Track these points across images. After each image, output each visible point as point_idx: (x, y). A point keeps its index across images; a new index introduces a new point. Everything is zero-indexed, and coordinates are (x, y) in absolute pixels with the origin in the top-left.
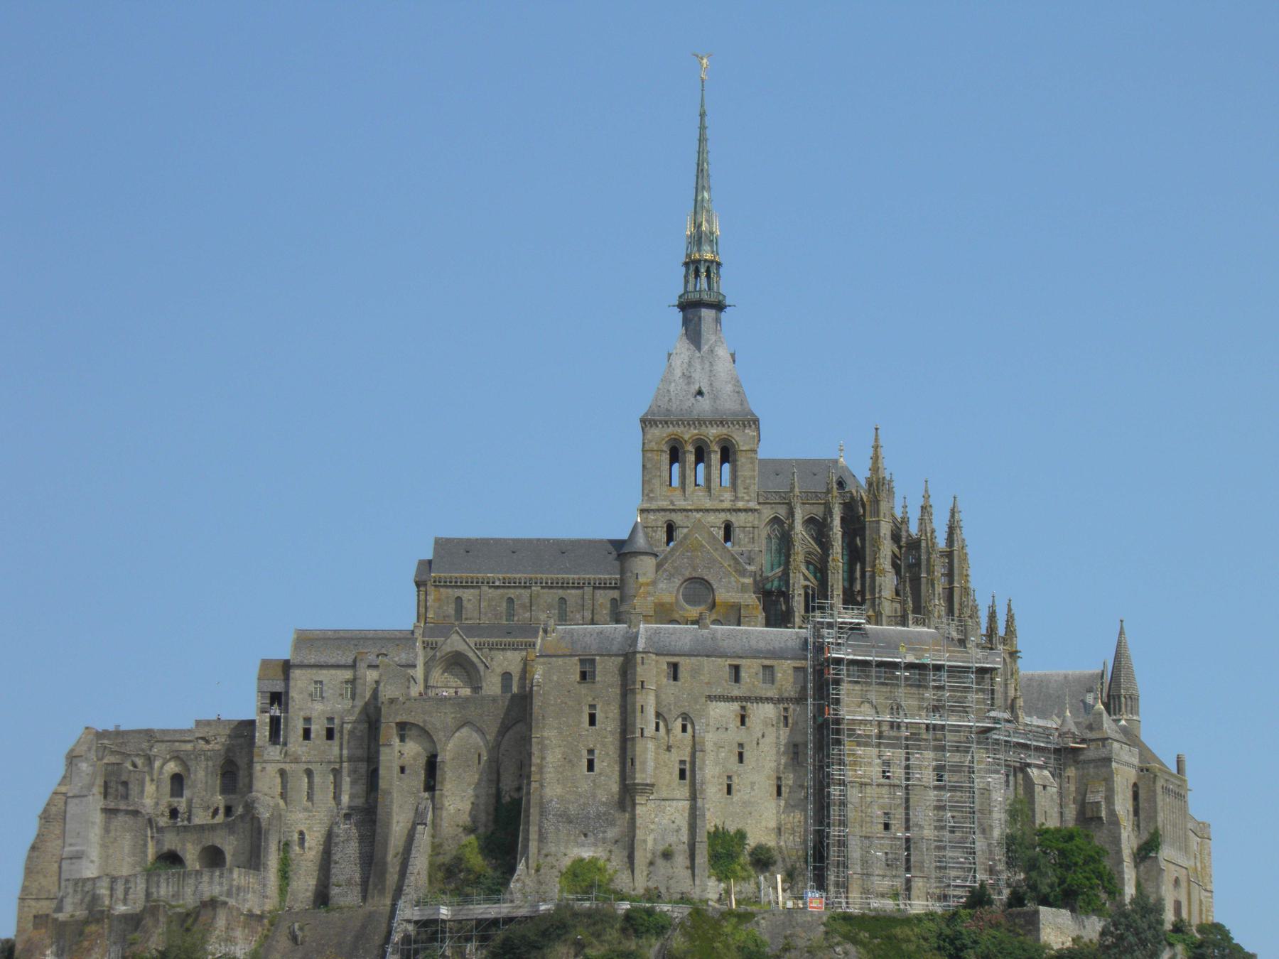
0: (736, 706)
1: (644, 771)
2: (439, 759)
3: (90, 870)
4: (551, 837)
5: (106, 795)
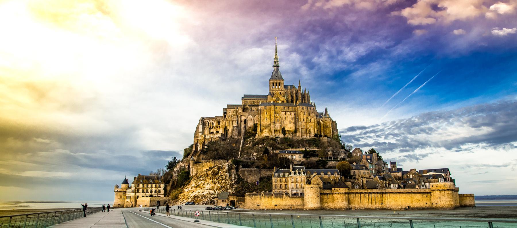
0: (285, 112)
4: (262, 129)
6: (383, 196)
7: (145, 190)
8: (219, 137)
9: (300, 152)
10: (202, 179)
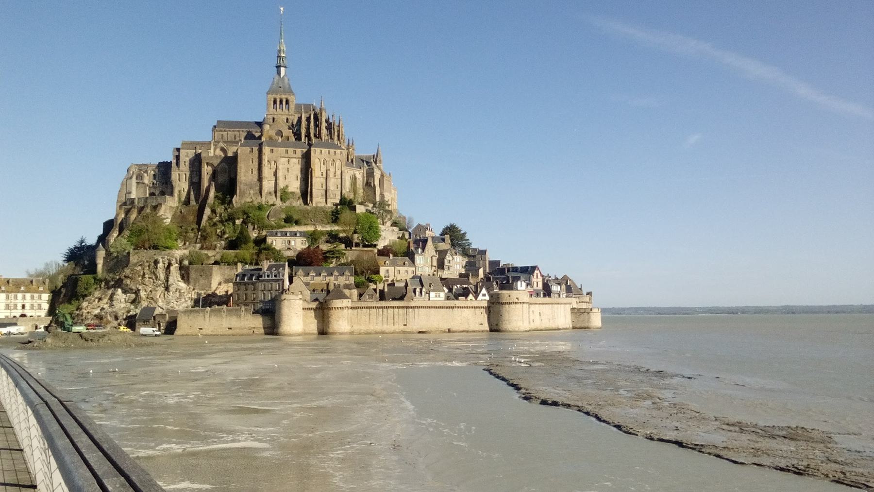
0: (287, 159)
1: (264, 174)
3: (133, 196)
5: (137, 179)
6: (408, 311)
7: (12, 305)
9: (303, 234)
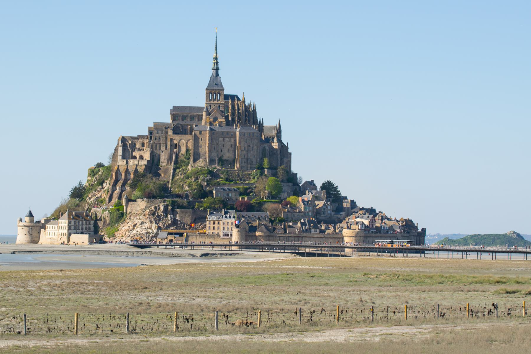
0: (223, 138)
2: (177, 144)
8: (146, 165)
10: (138, 218)
